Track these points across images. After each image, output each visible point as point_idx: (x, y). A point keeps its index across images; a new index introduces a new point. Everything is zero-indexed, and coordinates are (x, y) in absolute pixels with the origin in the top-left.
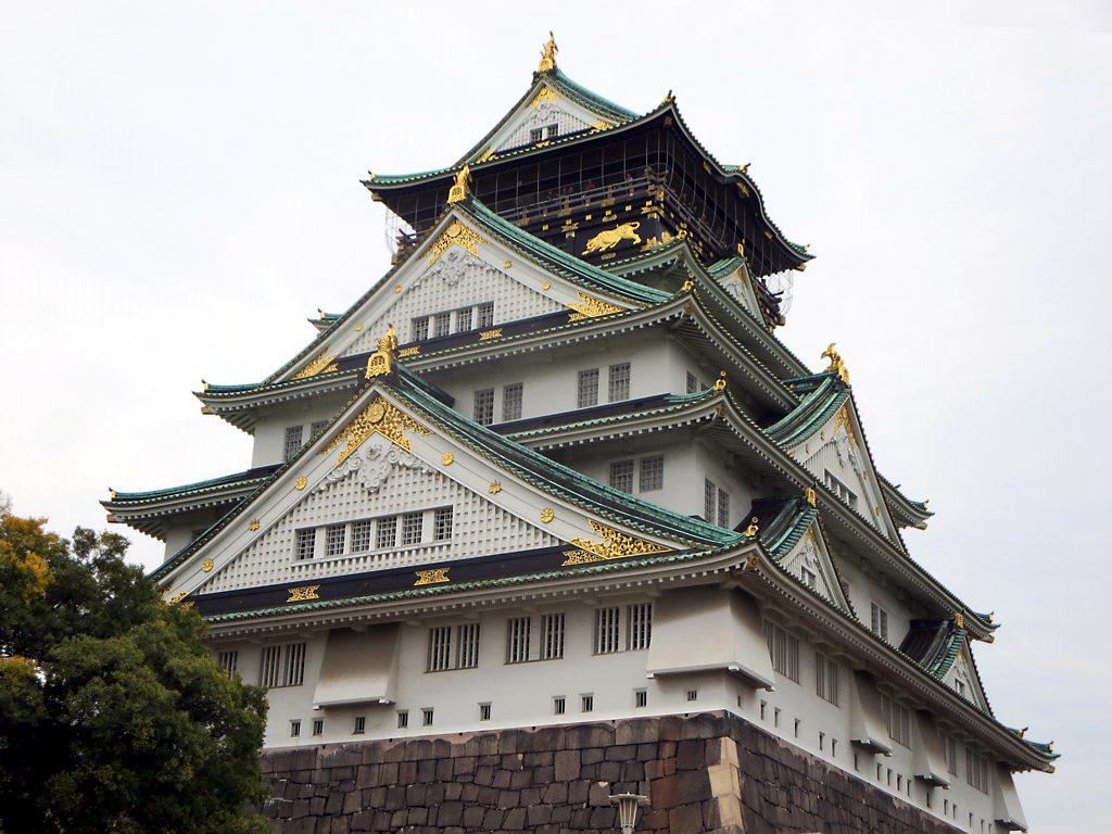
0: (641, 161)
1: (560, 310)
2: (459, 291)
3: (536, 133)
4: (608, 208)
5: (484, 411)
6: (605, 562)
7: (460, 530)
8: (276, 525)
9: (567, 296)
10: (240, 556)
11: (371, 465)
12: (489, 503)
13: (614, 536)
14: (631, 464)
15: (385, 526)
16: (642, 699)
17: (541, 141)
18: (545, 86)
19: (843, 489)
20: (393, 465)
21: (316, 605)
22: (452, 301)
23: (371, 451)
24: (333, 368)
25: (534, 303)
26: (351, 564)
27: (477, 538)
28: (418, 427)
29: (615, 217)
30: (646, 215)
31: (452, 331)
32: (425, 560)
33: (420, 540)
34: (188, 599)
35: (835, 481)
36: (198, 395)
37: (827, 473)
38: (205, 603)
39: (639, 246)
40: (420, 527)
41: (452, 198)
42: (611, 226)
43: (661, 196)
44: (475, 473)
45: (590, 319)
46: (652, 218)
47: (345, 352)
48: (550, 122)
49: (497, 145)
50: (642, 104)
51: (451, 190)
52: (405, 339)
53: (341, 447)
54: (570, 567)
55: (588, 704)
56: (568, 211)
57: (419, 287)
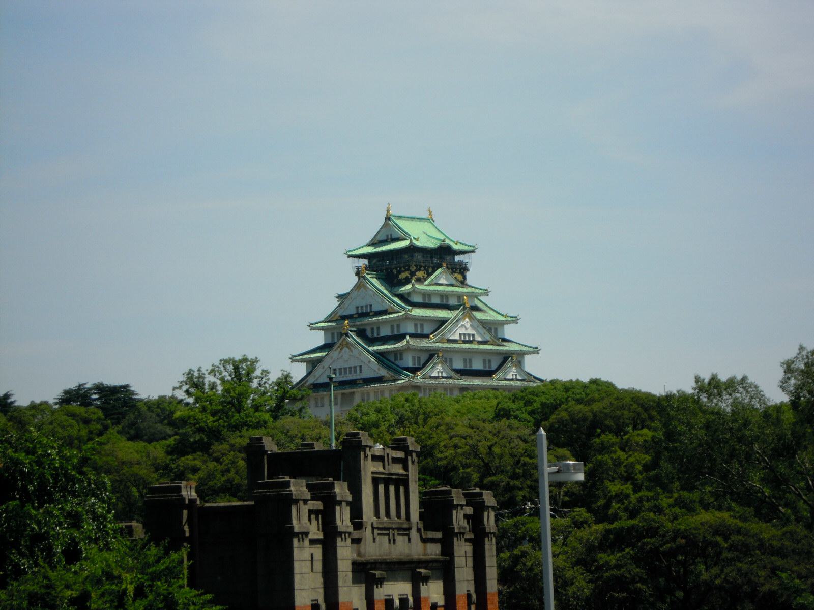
3: (387, 236)
5: (373, 333)
19: (469, 335)
24: (339, 318)
27: (367, 374)
34: (312, 384)
35: (465, 335)
37: (460, 334)
38: (317, 387)
42: (404, 272)
52: (355, 312)
53: (339, 349)
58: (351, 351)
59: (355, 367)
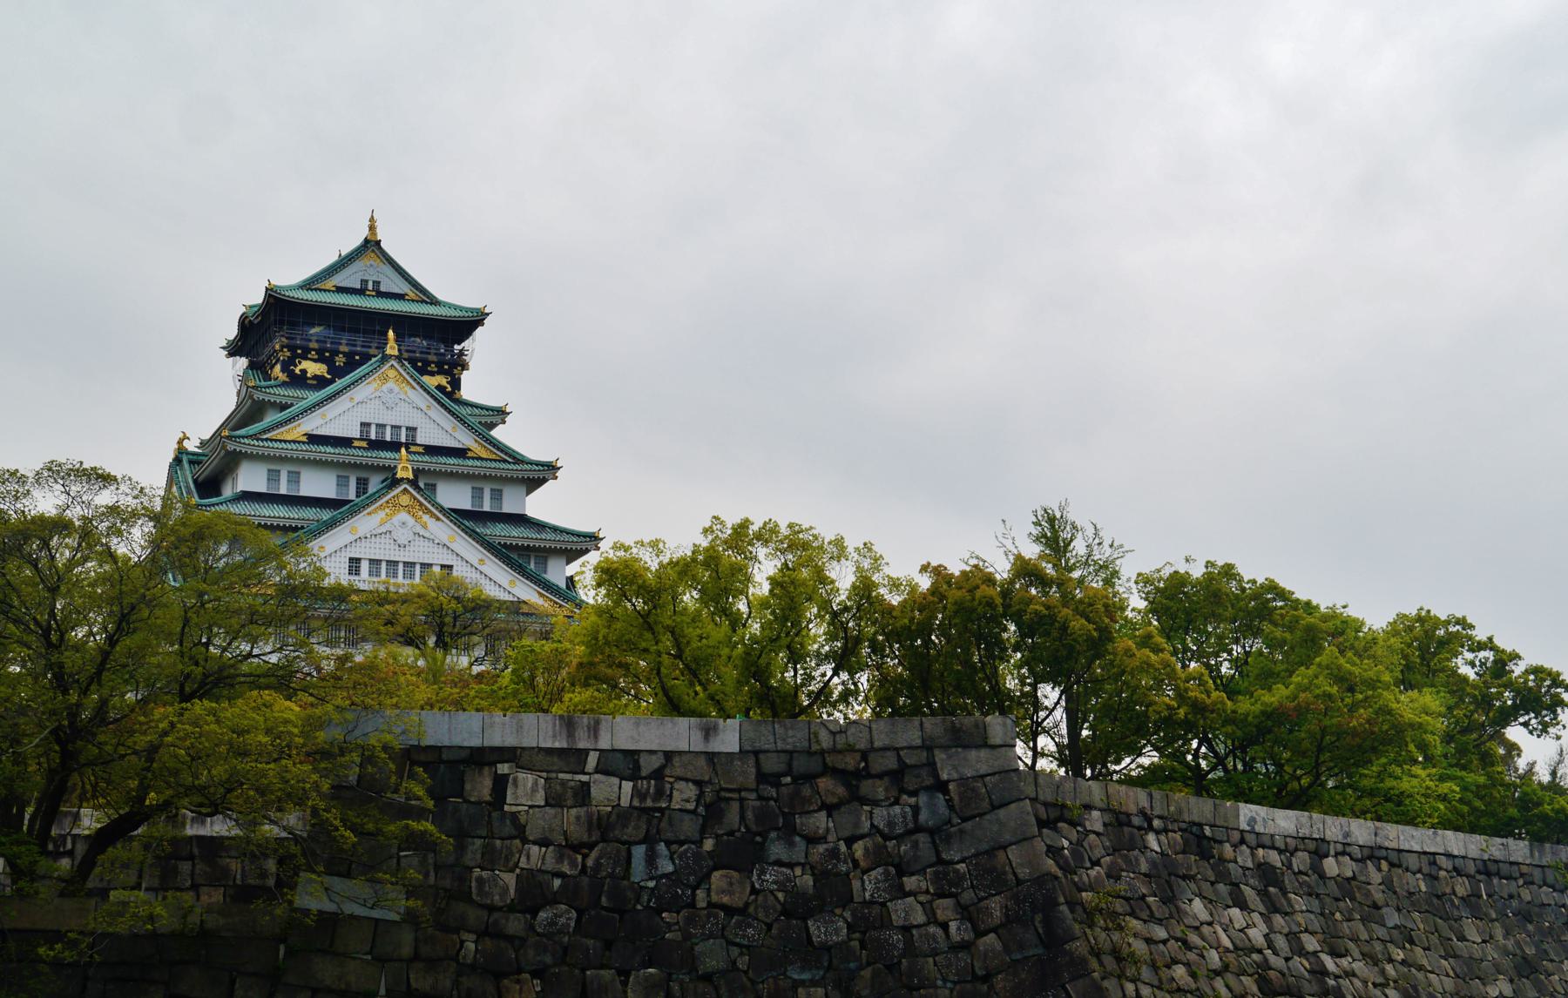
3: (364, 282)
28: (433, 515)
31: (388, 438)
41: (389, 351)
42: (432, 374)
44: (470, 551)
49: (341, 279)
58: (425, 527)
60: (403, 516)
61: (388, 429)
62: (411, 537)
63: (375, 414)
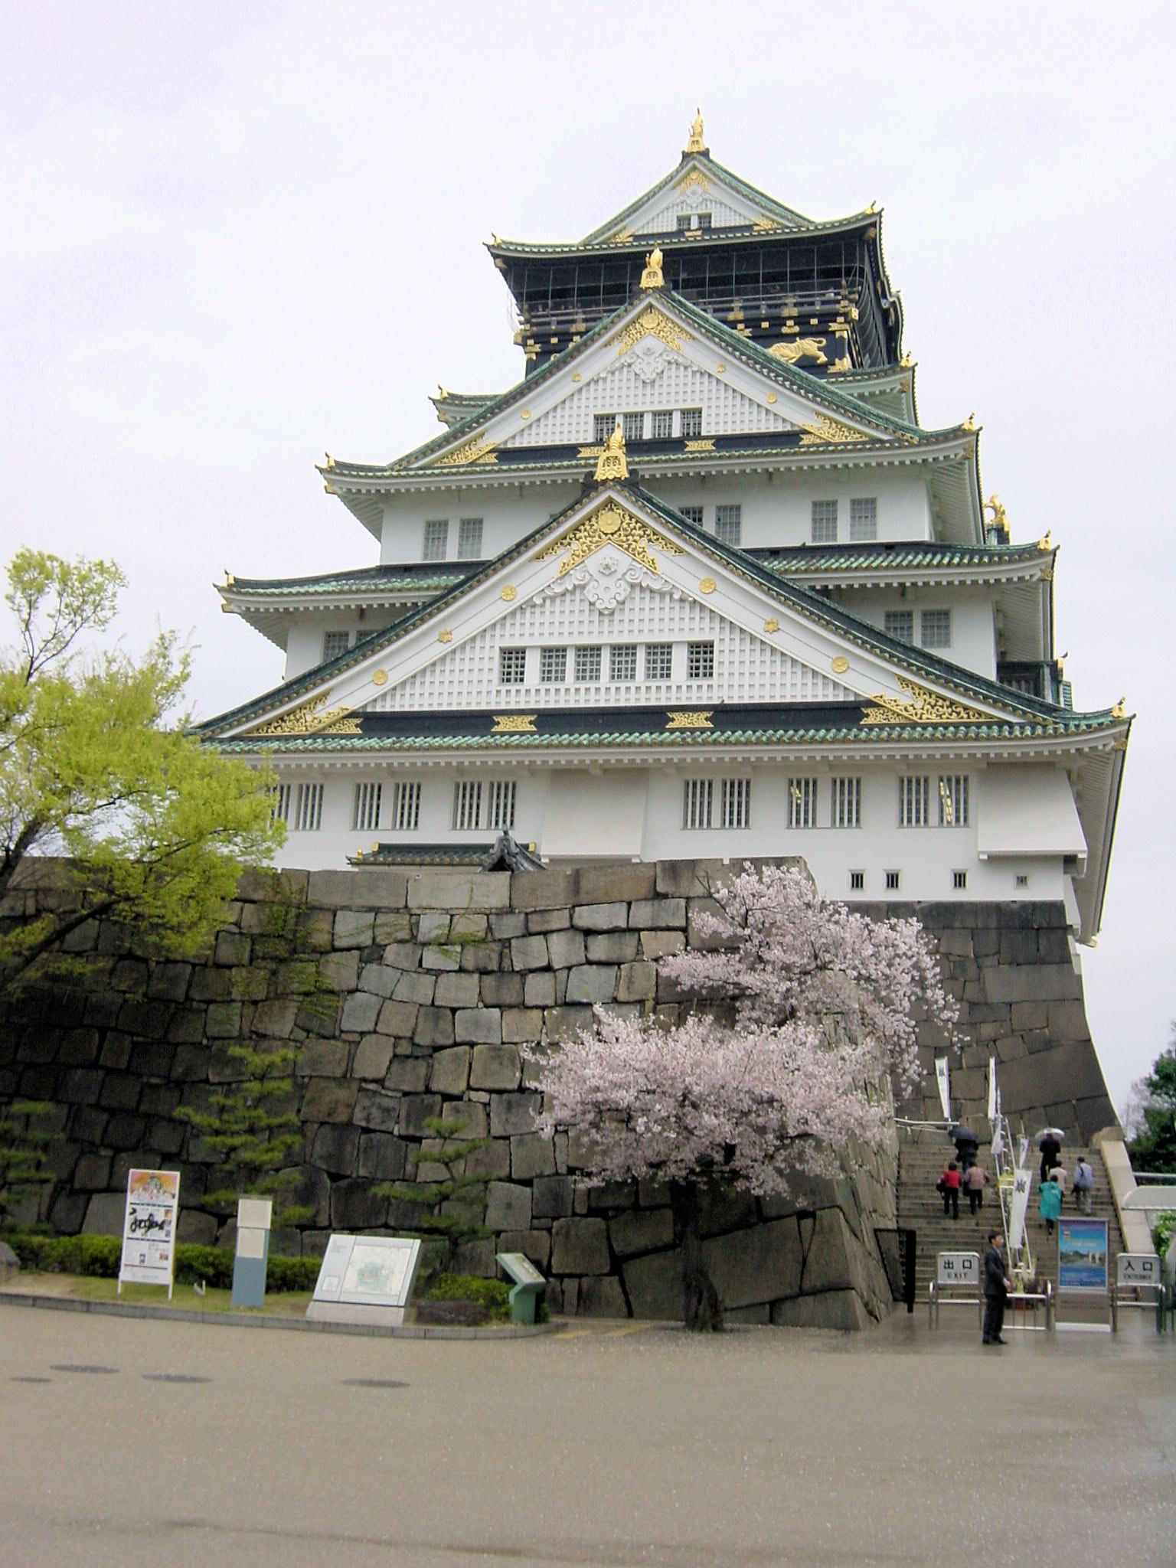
0: (837, 273)
1: (789, 428)
2: (657, 391)
3: (684, 220)
4: (790, 318)
6: (914, 726)
7: (726, 669)
8: (473, 639)
9: (792, 412)
10: (424, 671)
11: (604, 582)
12: (762, 642)
13: (927, 697)
14: (910, 614)
15: (620, 655)
16: (960, 880)
17: (689, 230)
18: (695, 168)
20: (632, 586)
21: (526, 740)
22: (647, 402)
23: (607, 567)
24: (492, 458)
25: (755, 417)
26: (572, 693)
27: (742, 680)
29: (797, 329)
30: (834, 332)
31: (647, 435)
32: (668, 699)
33: (668, 676)
34: (353, 715)
36: (321, 470)
38: (374, 723)
39: (825, 366)
40: (669, 661)
42: (790, 338)
43: (855, 314)
45: (829, 444)
46: (842, 337)
47: (506, 442)
48: (702, 211)
50: (824, 208)
51: (645, 273)
53: (564, 555)
54: (871, 727)
55: (893, 880)
56: (740, 315)
57: (605, 379)
59: (660, 651)
60: (611, 553)
61: (648, 420)
62: (623, 591)
63: (620, 398)
